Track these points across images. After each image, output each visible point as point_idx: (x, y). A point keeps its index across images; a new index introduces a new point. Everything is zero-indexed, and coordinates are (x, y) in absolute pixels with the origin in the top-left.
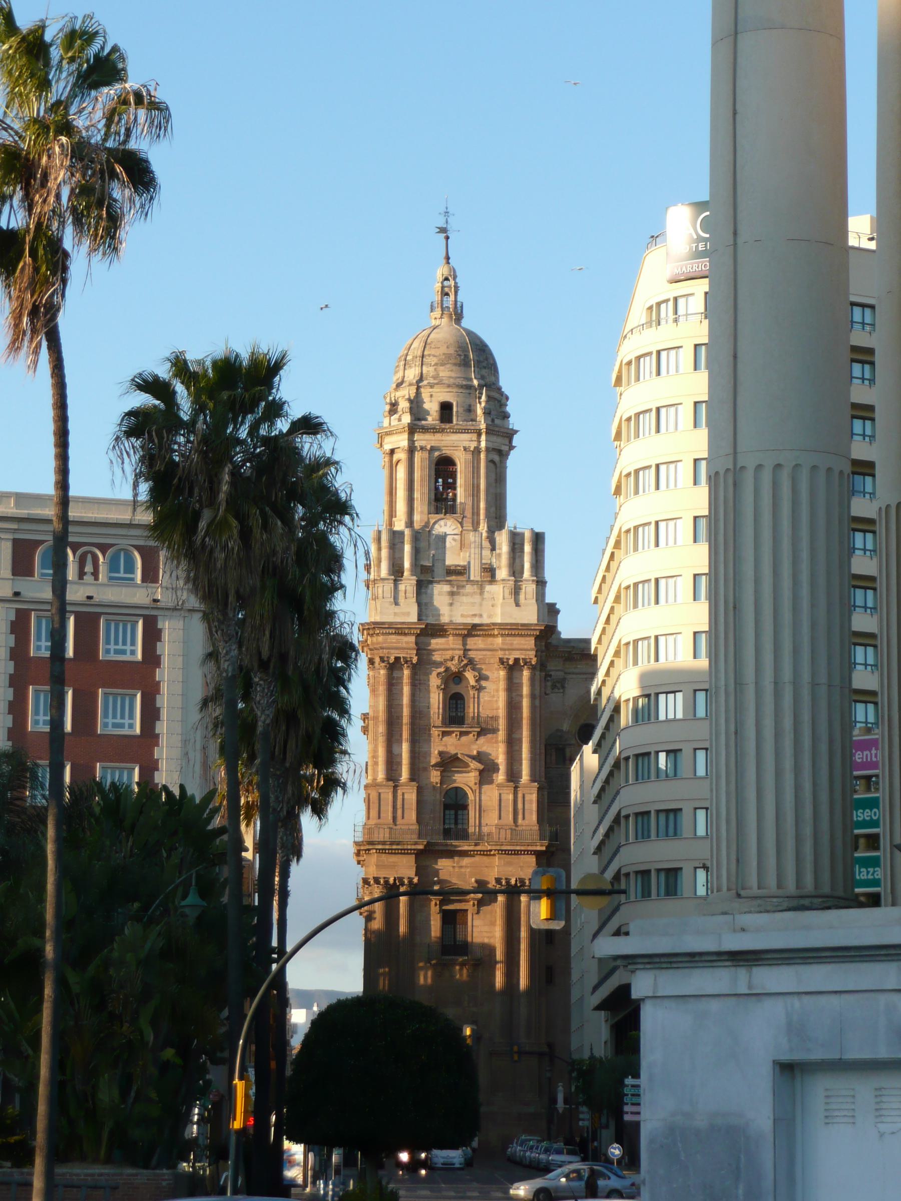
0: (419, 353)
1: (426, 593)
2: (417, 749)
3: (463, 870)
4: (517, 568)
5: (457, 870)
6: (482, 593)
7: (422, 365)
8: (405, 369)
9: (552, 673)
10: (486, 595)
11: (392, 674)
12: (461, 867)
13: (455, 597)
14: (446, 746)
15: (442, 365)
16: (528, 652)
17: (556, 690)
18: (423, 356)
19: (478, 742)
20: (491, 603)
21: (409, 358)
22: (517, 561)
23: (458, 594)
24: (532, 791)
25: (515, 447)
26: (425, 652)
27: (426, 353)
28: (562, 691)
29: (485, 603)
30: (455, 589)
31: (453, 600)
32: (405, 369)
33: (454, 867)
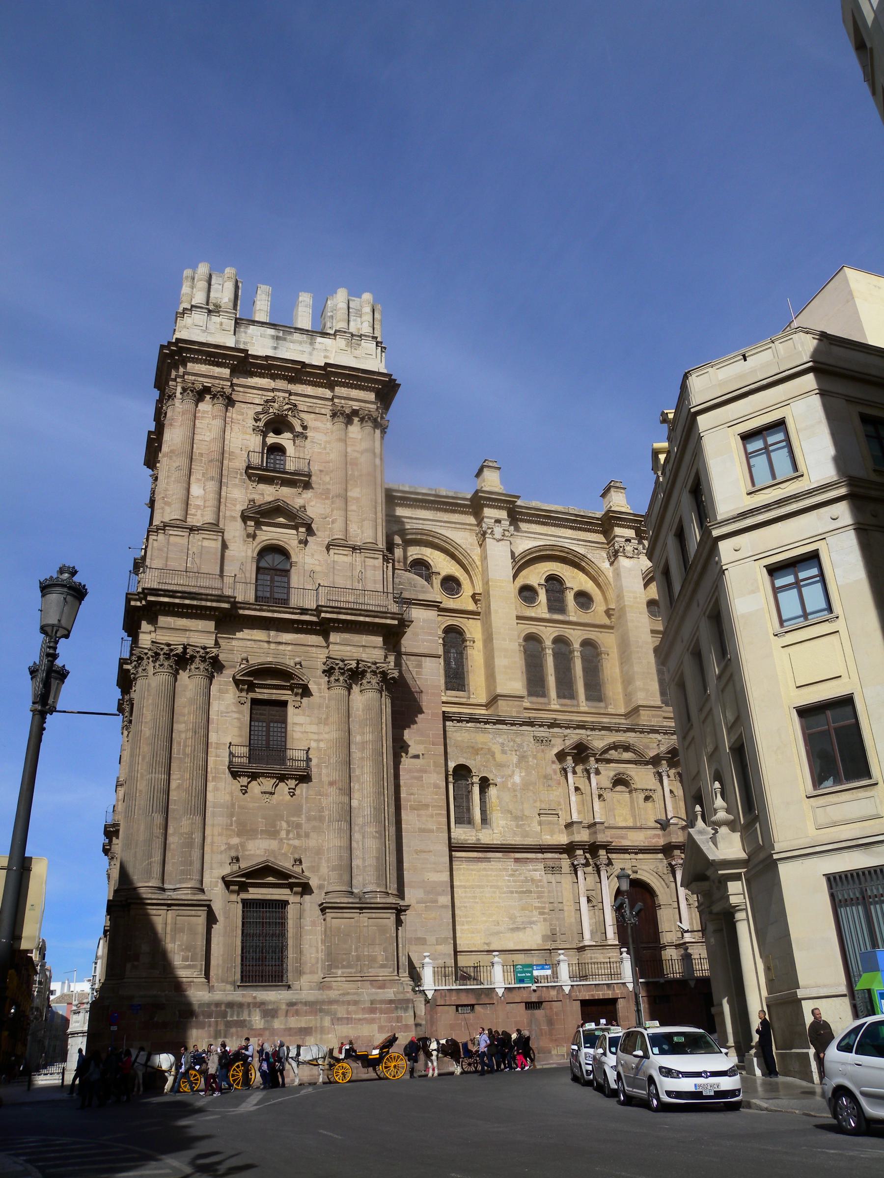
1: (246, 333)
6: (312, 344)
10: (317, 346)
11: (197, 406)
13: (281, 342)
14: (263, 494)
19: (304, 496)
23: (285, 339)
24: (376, 556)
29: (315, 352)
30: (281, 334)
31: (278, 344)
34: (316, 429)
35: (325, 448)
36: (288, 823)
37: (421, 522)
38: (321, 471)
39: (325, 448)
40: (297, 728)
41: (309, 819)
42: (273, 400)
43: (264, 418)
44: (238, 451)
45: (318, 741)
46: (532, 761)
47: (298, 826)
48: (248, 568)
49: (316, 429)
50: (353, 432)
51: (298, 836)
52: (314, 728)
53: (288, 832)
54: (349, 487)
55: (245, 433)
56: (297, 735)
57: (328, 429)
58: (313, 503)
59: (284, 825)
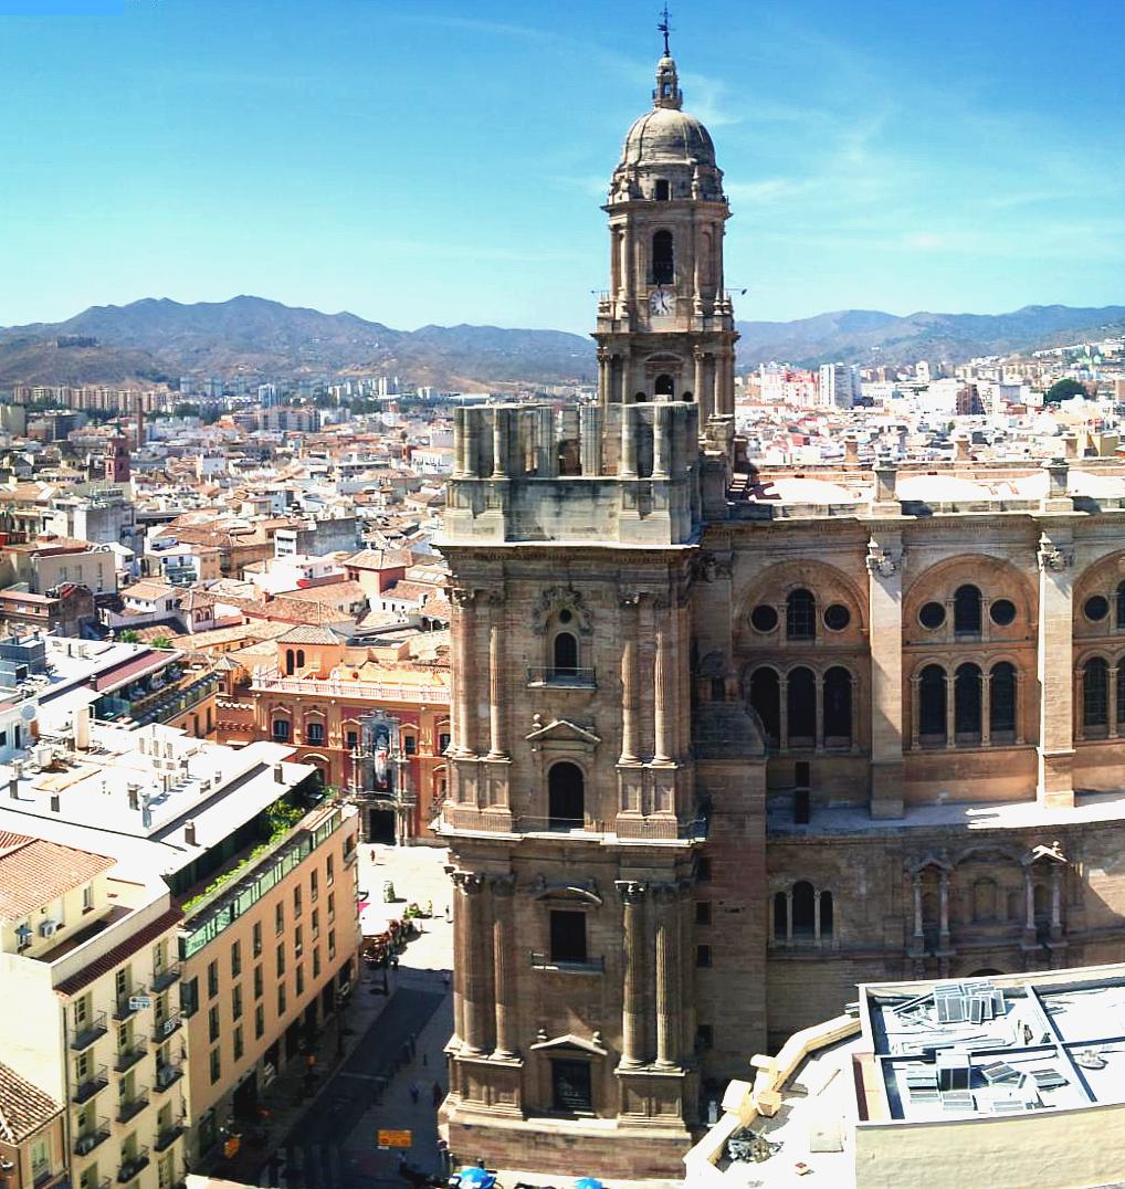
0: (639, 136)
2: (509, 713)
3: (576, 867)
4: (645, 460)
5: (568, 865)
7: (641, 147)
8: (627, 151)
9: (717, 555)
11: (475, 611)
12: (574, 862)
15: (658, 146)
16: (658, 586)
17: (722, 576)
18: (641, 139)
19: (593, 705)
20: (607, 512)
21: (631, 141)
22: (645, 448)
25: (731, 215)
26: (518, 582)
27: (644, 136)
28: (728, 576)
32: (627, 151)
33: (563, 862)
34: (601, 619)
35: (614, 642)
36: (589, 1008)
37: (799, 551)
38: (611, 672)
39: (614, 642)
40: (594, 936)
41: (607, 1006)
42: (553, 590)
43: (544, 615)
44: (520, 660)
45: (614, 945)
46: (880, 873)
47: (598, 1011)
48: (540, 789)
49: (601, 619)
50: (645, 619)
51: (599, 1018)
52: (610, 935)
53: (589, 1016)
54: (643, 689)
55: (527, 636)
56: (594, 942)
57: (616, 619)
58: (603, 712)
59: (586, 1009)
